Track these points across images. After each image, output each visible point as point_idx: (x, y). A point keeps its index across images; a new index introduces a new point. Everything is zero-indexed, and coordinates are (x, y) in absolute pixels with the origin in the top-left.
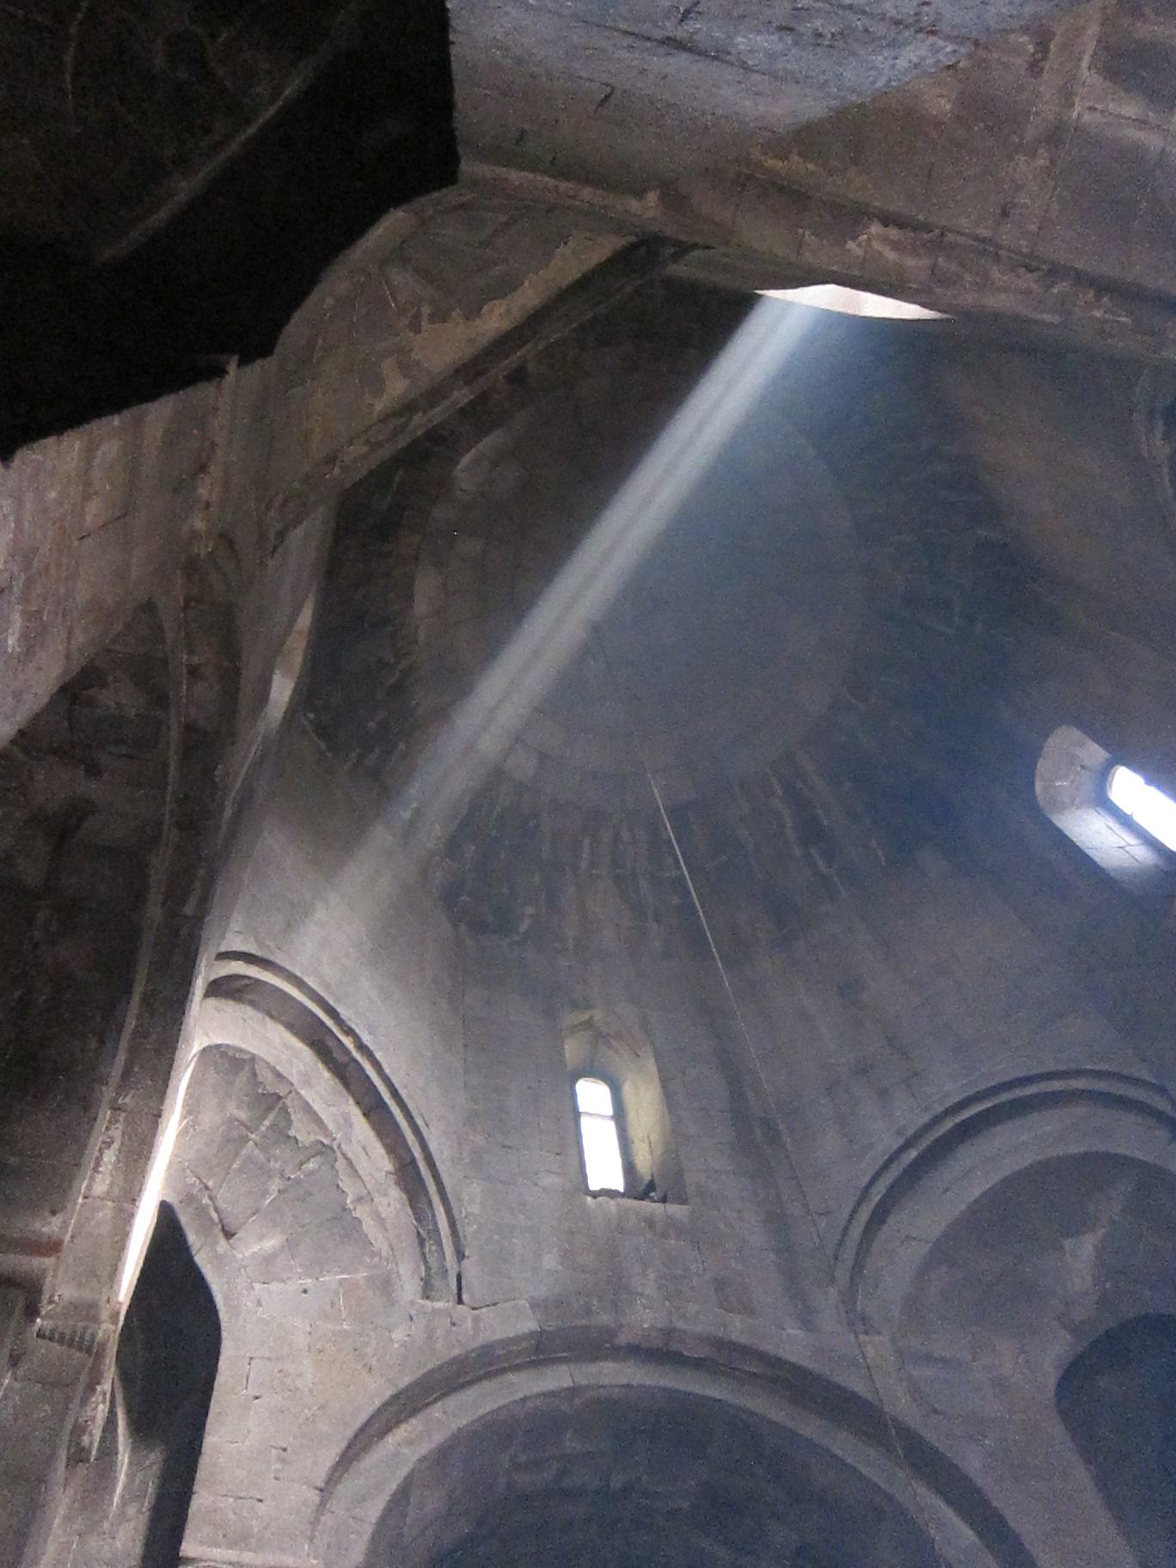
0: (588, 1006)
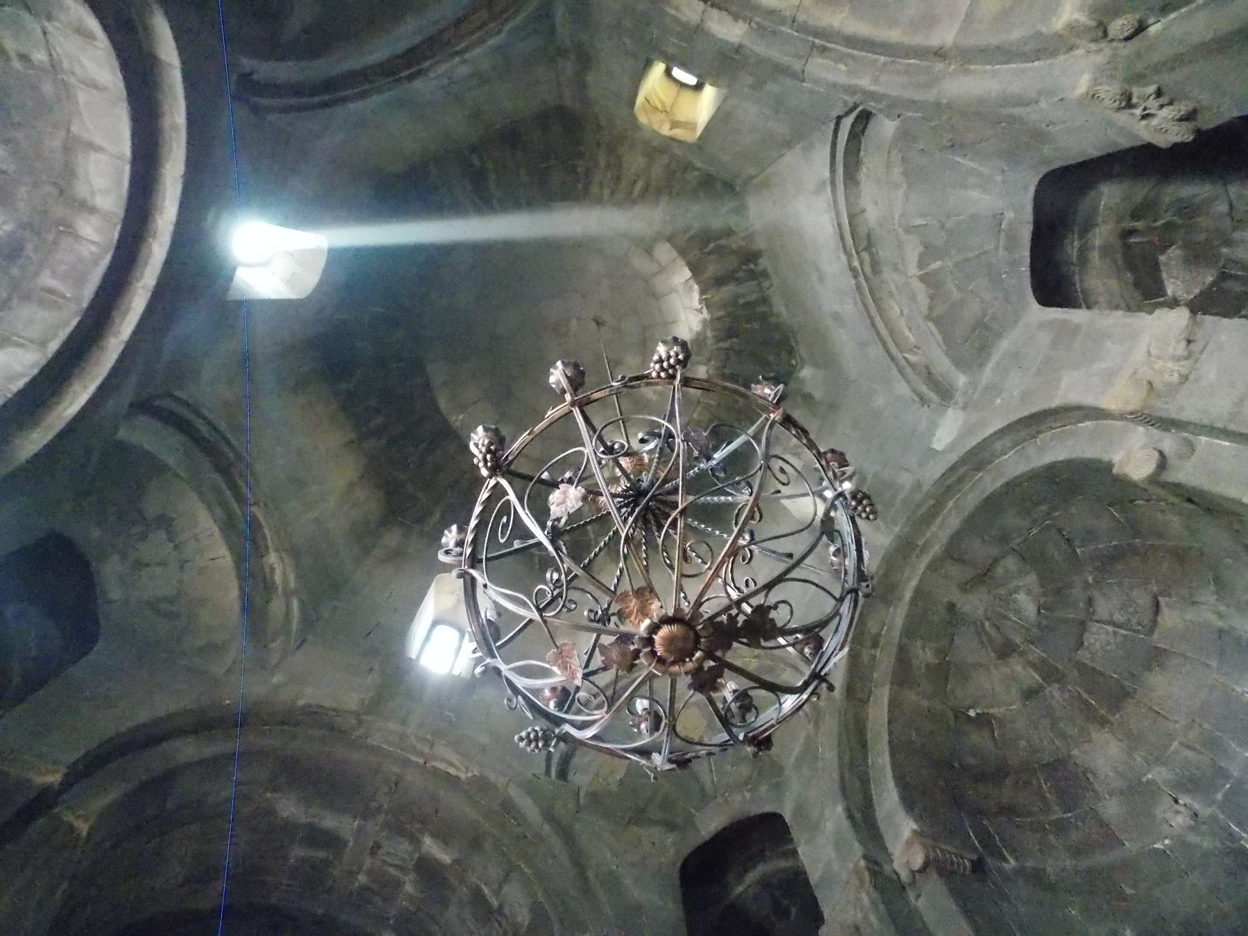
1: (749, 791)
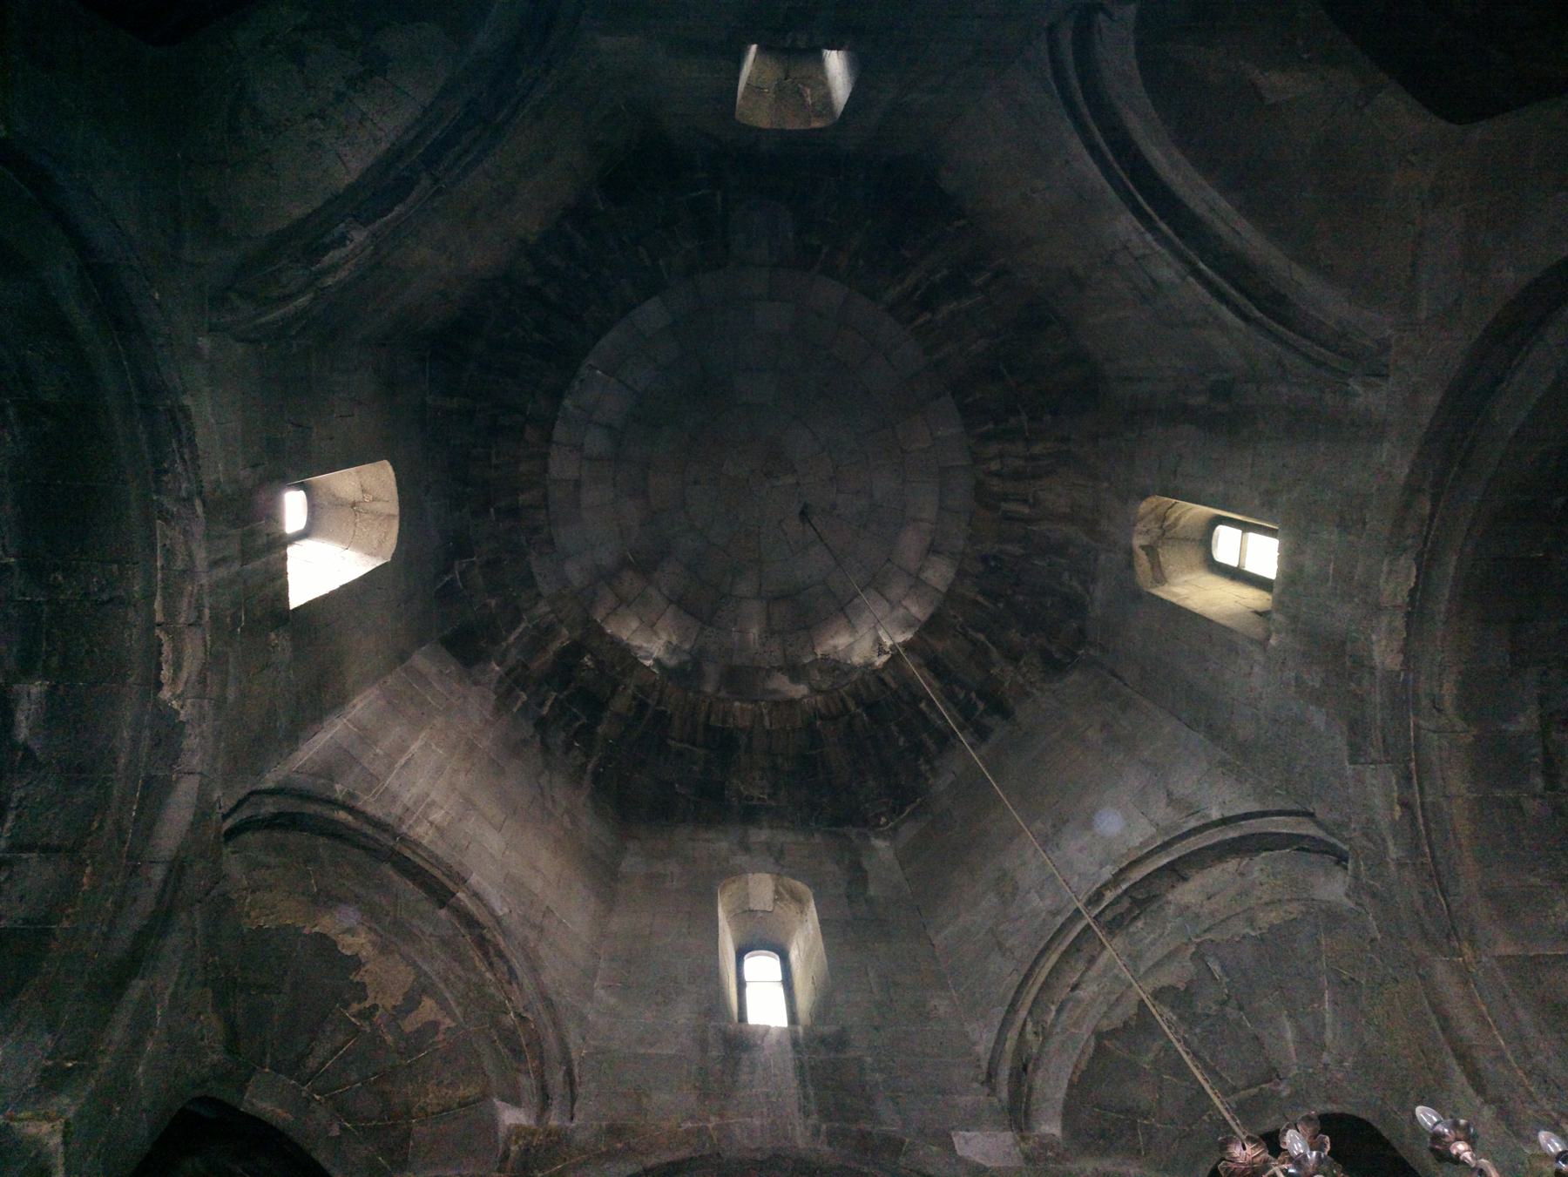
0: (1130, 552)
1: (343, 1129)
